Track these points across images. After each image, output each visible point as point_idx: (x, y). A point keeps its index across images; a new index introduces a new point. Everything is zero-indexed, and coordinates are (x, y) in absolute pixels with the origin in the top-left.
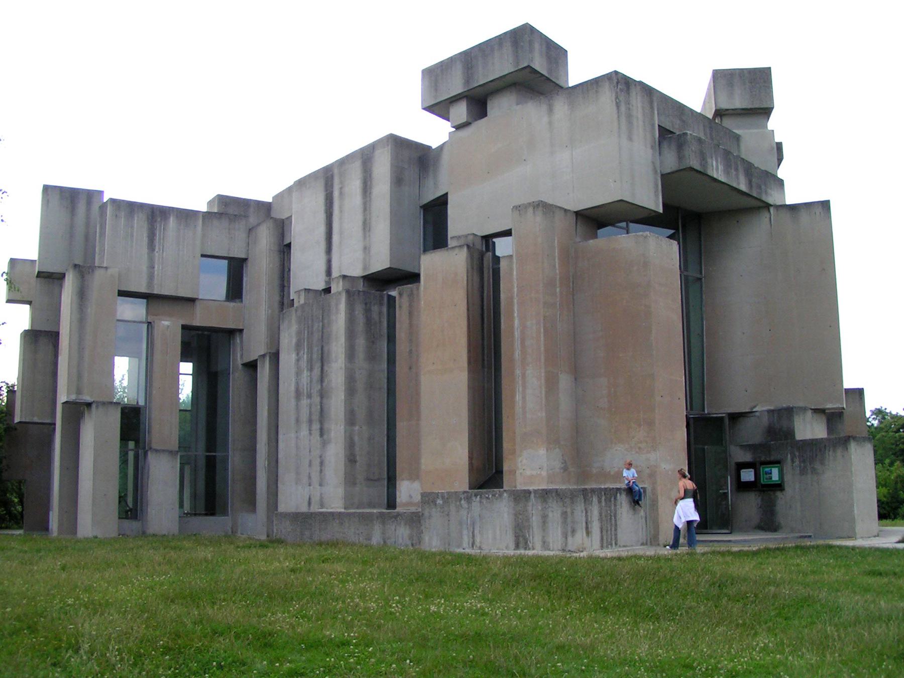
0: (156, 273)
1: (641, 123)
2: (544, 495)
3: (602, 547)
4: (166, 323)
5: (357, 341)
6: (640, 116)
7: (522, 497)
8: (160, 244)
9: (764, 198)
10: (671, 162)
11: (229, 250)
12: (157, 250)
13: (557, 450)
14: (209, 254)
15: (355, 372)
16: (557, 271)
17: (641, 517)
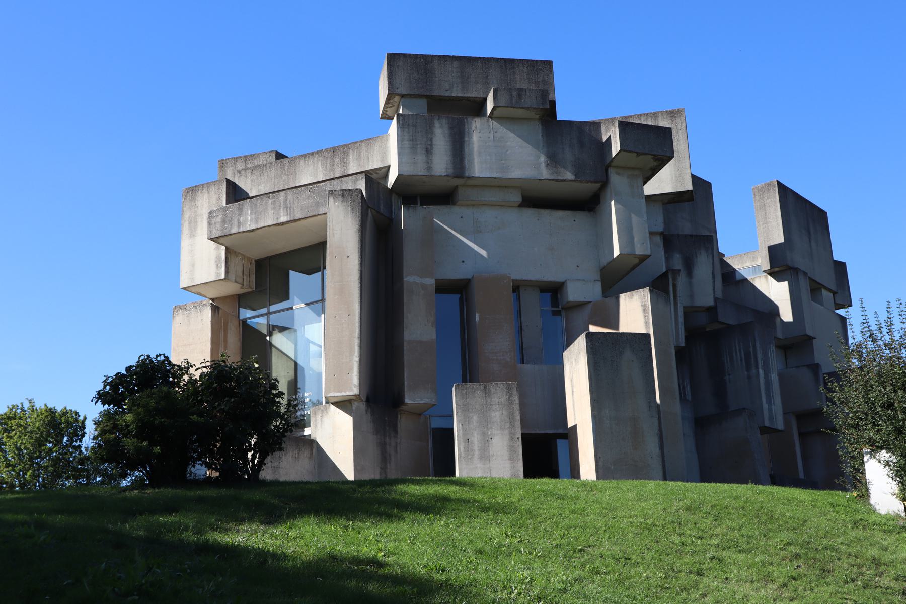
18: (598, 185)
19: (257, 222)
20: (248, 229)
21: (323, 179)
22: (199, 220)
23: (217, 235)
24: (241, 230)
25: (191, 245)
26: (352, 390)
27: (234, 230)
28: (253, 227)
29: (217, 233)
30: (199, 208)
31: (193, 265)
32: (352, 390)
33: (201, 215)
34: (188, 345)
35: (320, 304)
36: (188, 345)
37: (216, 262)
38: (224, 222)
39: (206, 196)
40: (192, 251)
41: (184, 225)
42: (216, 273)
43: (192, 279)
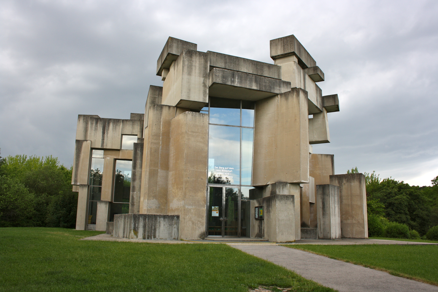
0: (105, 141)
1: (197, 68)
2: (145, 216)
3: (144, 238)
4: (108, 158)
5: (137, 161)
6: (197, 65)
7: (136, 218)
8: (107, 131)
9: (272, 91)
10: (209, 83)
11: (132, 132)
12: (106, 133)
13: (154, 200)
14: (125, 134)
15: (136, 173)
16: (161, 130)
17: (174, 227)
18: (319, 112)
19: (241, 82)
20: (236, 85)
21: (252, 73)
22: (194, 68)
23: (220, 83)
24: (233, 84)
25: (188, 79)
26: (308, 181)
27: (229, 83)
28: (238, 85)
29: (219, 81)
30: (194, 62)
31: (190, 90)
32: (308, 181)
33: (195, 66)
34: (195, 132)
35: (239, 128)
36: (195, 132)
37: (203, 93)
38: (223, 77)
39: (198, 58)
40: (189, 82)
41: (184, 67)
42: (203, 98)
43: (189, 97)
